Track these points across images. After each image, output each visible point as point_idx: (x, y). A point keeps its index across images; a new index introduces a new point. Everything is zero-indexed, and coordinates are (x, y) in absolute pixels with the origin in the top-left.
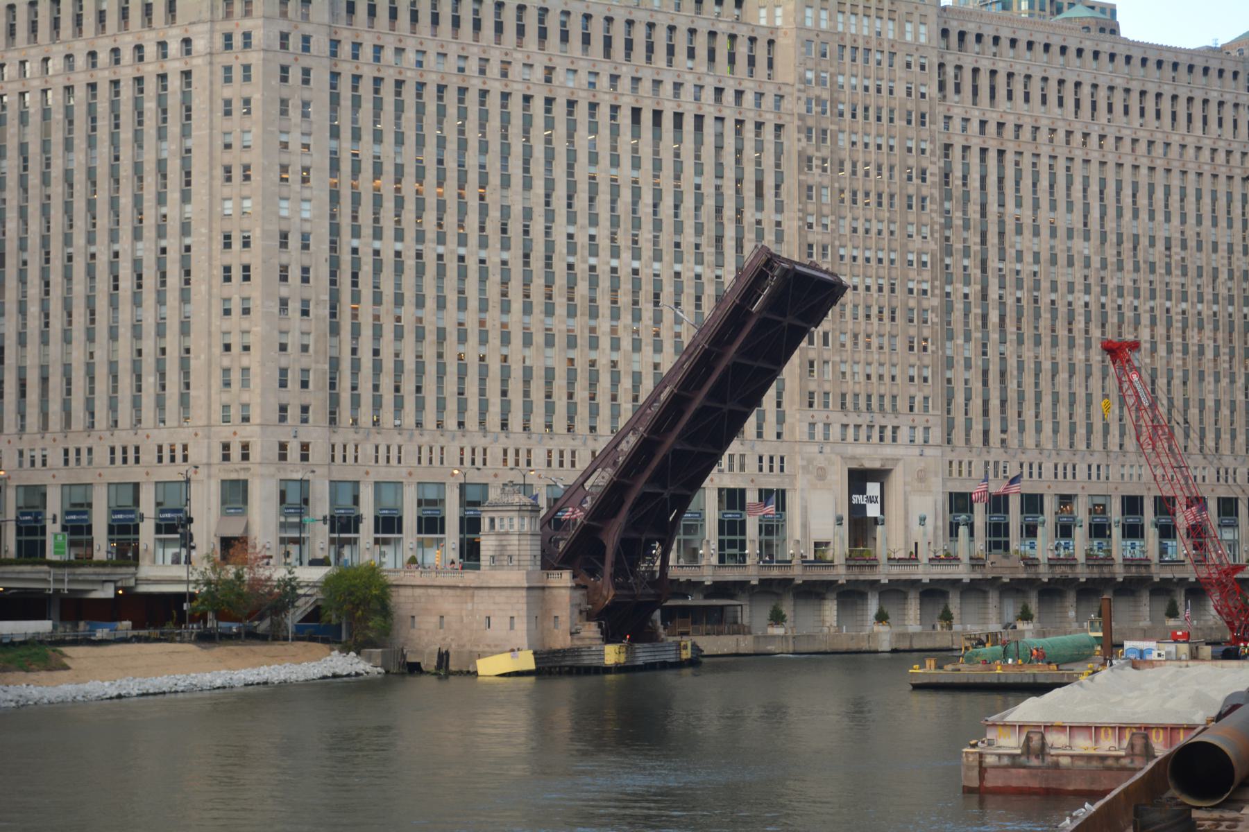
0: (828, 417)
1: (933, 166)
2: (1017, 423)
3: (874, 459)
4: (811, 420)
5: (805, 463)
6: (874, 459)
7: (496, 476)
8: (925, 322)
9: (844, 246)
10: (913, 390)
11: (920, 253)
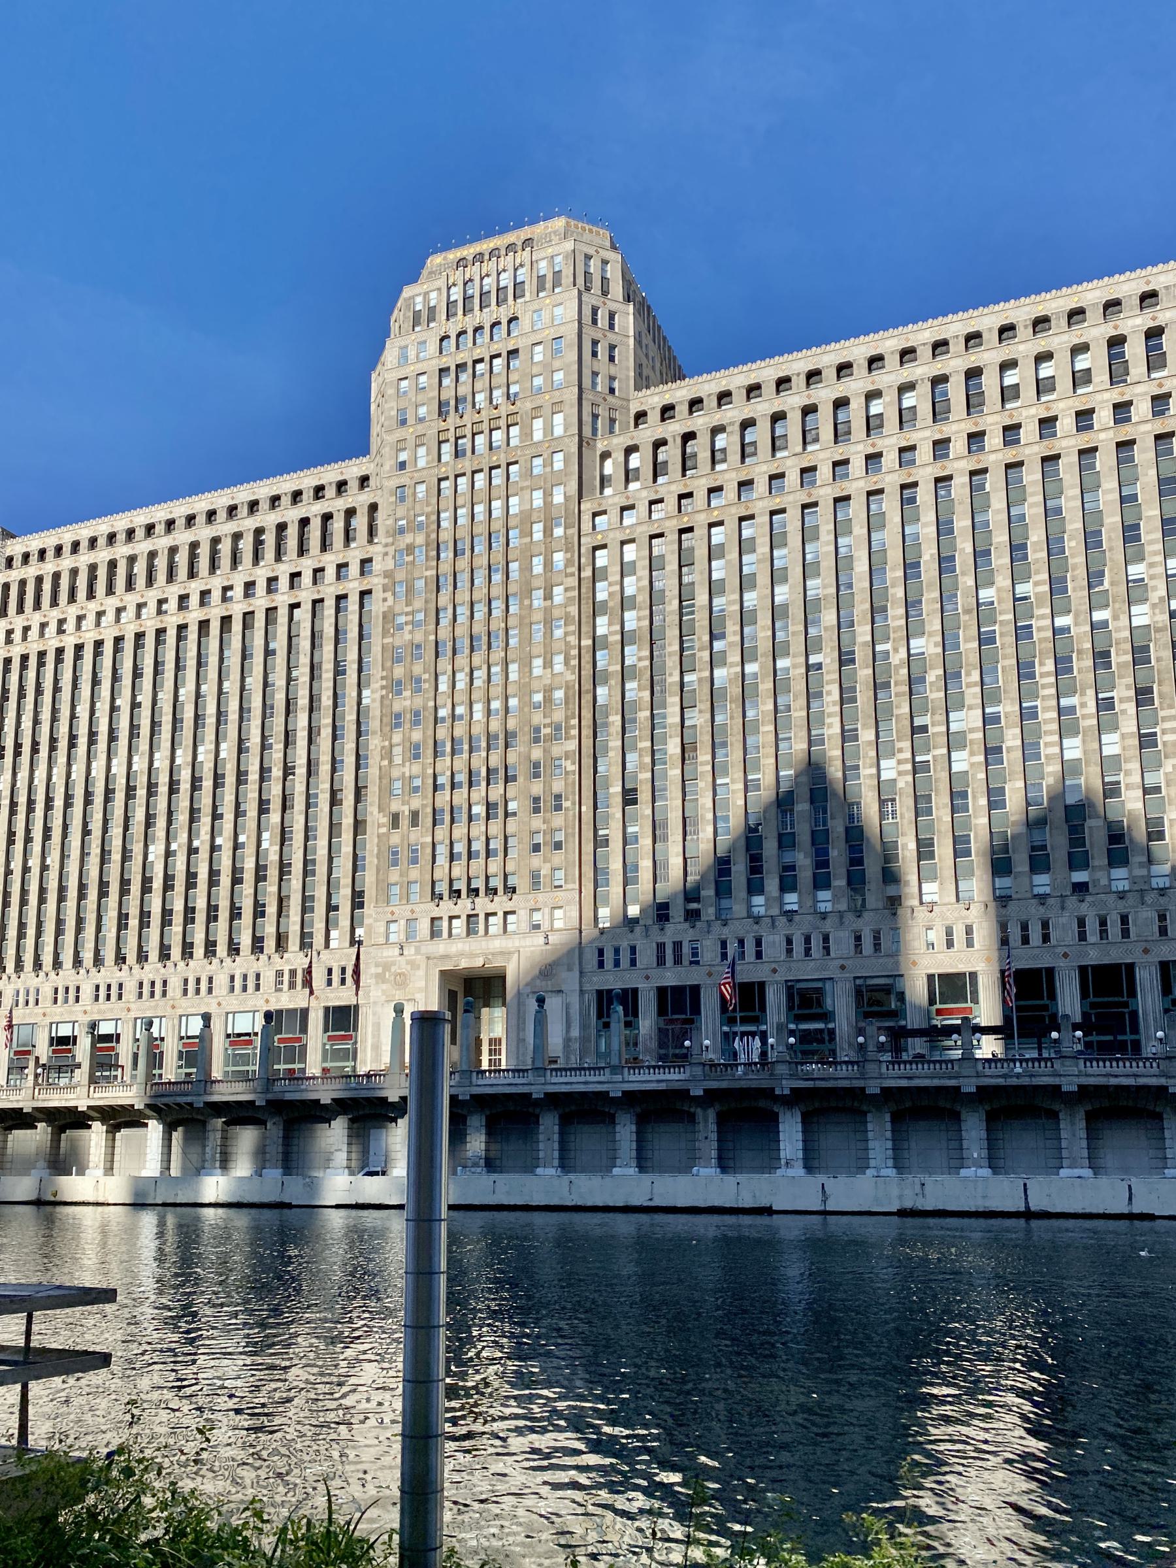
0: (413, 912)
1: (570, 579)
2: (713, 886)
3: (477, 955)
4: (389, 917)
5: (380, 970)
6: (477, 955)
9: (444, 706)
10: (536, 861)
11: (548, 691)
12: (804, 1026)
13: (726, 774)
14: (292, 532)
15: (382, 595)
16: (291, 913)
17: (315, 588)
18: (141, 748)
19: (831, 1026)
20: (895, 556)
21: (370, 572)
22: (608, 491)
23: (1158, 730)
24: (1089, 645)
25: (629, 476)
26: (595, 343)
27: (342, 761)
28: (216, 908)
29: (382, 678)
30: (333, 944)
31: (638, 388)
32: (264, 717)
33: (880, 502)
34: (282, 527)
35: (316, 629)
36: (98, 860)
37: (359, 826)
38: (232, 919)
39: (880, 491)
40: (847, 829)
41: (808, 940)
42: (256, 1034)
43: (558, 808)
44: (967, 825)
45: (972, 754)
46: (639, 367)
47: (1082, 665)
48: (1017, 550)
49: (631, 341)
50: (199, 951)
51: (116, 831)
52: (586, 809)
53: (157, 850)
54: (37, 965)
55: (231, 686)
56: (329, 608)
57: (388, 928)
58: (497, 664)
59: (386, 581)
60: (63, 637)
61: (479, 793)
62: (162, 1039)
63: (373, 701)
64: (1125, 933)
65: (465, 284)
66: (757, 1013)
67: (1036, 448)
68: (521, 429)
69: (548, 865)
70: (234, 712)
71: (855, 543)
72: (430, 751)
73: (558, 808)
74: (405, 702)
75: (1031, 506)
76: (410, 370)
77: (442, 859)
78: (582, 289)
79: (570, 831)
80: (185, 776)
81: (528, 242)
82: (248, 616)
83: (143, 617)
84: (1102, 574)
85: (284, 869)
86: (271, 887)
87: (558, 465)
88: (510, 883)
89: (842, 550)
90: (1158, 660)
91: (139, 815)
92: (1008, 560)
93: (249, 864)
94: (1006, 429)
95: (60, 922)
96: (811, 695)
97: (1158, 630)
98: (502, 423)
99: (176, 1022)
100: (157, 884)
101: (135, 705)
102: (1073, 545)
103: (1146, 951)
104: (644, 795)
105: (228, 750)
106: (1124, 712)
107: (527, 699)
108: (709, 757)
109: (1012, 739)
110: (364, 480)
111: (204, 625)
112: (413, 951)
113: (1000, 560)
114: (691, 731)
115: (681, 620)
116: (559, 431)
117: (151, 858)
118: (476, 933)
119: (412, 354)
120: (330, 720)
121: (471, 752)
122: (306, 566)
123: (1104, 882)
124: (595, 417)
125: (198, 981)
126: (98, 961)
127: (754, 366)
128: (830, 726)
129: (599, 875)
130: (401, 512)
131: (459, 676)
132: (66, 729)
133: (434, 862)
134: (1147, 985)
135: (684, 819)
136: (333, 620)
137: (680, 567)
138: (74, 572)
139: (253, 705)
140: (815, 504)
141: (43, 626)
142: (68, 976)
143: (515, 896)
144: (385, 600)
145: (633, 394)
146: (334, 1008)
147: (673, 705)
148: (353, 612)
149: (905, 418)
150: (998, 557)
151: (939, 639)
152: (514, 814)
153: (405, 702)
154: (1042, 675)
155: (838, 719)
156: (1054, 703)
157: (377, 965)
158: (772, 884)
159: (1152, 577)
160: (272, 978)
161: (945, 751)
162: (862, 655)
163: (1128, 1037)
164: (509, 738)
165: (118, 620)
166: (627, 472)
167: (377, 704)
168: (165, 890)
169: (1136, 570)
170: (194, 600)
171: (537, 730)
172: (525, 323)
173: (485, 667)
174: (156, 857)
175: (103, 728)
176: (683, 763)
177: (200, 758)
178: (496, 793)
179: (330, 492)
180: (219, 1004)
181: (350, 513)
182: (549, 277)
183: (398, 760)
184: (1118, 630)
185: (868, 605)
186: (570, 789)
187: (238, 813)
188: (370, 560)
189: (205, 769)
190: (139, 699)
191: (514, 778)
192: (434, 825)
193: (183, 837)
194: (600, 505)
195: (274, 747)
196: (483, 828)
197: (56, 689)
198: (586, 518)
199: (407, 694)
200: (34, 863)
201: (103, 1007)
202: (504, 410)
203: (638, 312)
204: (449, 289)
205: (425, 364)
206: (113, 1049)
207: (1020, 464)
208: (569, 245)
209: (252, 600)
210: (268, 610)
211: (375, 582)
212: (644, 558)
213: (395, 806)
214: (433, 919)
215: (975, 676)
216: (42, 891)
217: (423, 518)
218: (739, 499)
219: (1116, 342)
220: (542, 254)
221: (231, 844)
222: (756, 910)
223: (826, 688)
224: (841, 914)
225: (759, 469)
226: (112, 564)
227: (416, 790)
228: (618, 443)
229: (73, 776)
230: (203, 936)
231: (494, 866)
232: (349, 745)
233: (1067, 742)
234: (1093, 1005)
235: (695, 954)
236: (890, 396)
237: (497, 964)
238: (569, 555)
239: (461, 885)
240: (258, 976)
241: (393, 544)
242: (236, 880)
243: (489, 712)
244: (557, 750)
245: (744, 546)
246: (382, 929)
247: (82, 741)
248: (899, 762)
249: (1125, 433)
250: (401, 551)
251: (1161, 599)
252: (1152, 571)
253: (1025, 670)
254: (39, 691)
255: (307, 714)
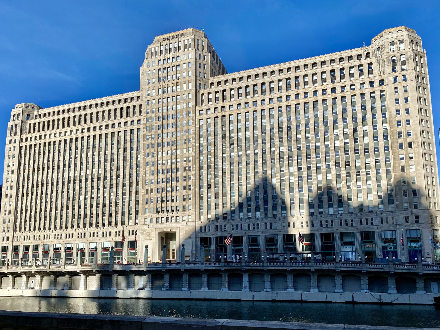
0: (151, 216)
1: (193, 128)
3: (169, 228)
4: (145, 217)
5: (143, 231)
6: (169, 228)
7: (52, 242)
8: (190, 179)
10: (184, 203)
12: (253, 247)
13: (233, 181)
14: (119, 111)
15: (143, 130)
16: (119, 216)
17: (125, 127)
18: (77, 170)
19: (259, 247)
20: (276, 126)
21: (140, 123)
22: (203, 104)
23: (341, 173)
24: (324, 151)
25: (209, 100)
26: (200, 64)
27: (132, 175)
28: (99, 213)
29: (143, 153)
30: (130, 224)
31: (211, 76)
32: (111, 162)
33: (273, 111)
34: (116, 110)
35: (125, 138)
36: (66, 200)
37: (137, 192)
38: (103, 217)
39: (273, 108)
40: (264, 196)
41: (254, 225)
42: (110, 248)
43: (190, 189)
44: (293, 196)
45: (295, 178)
46: (212, 70)
47: (322, 156)
48: (307, 125)
49: (210, 63)
50: (94, 225)
51: (71, 192)
52: (198, 189)
53: (82, 198)
54: (50, 228)
55: (102, 153)
56: (129, 133)
57: (145, 220)
58: (174, 150)
59: (144, 126)
60: (55, 138)
61: (169, 184)
62: (84, 249)
63: (141, 158)
64: (332, 225)
65: (165, 45)
66: (241, 244)
67: (312, 99)
68: (180, 87)
69: (187, 204)
70: (103, 160)
71: (266, 121)
72: (156, 173)
73: (190, 189)
74: (149, 159)
75: (310, 114)
76: (150, 69)
77: (159, 202)
78: (197, 49)
79: (193, 195)
80: (90, 177)
81: (182, 35)
82: (107, 134)
83: (78, 133)
84: (328, 132)
85: (117, 204)
86: (113, 208)
87: (190, 97)
88: (177, 209)
89: (263, 123)
90: (341, 155)
91: (77, 188)
92: (304, 128)
93: (107, 202)
94: (304, 93)
95: (56, 217)
96: (255, 161)
97: (341, 147)
98: (175, 85)
99: (88, 244)
100: (82, 207)
101: (76, 157)
102: (321, 124)
103: (337, 230)
104: (213, 186)
105: (101, 170)
106: (332, 168)
107: (182, 159)
108: (229, 177)
109: (305, 174)
110: (138, 97)
111: (94, 136)
112: (151, 227)
113: (303, 128)
114: (224, 169)
115: (222, 140)
116: (190, 88)
117: (81, 199)
118: (168, 222)
119: (151, 64)
120: (129, 163)
121: (167, 173)
122: (123, 121)
123: (327, 212)
124: (200, 84)
125: (94, 233)
126: (67, 227)
127: (241, 72)
128: (260, 169)
129: (201, 207)
130: (148, 107)
131: (164, 153)
132: (57, 164)
133: (157, 202)
134: (337, 238)
135: (223, 192)
136: (130, 136)
137: (222, 126)
138: (58, 120)
139: (108, 159)
140: (256, 111)
141: (50, 135)
142: (58, 231)
143: (179, 212)
144: (144, 131)
145: (210, 78)
146: (131, 241)
147: (220, 162)
148: (135, 134)
149: (280, 88)
150: (302, 127)
151: (287, 148)
152: (179, 190)
153: (149, 159)
154: (313, 158)
155: (262, 168)
156: (315, 165)
157: (142, 230)
158: (245, 210)
159: (340, 134)
160: (114, 232)
161: (288, 177)
162: (268, 151)
163: (332, 251)
164: (177, 170)
165: (71, 134)
166: (208, 99)
167: (142, 159)
168: (85, 209)
169: (336, 132)
170: (92, 129)
171: (185, 168)
172: (181, 57)
173: (171, 150)
174: (82, 199)
175: (67, 164)
176: (223, 178)
177: (94, 173)
178: (174, 184)
179: (129, 100)
180: (100, 240)
181: (134, 107)
182: (188, 45)
183: (147, 175)
184: (331, 147)
185: (269, 138)
186: (193, 184)
187: (104, 188)
188: (140, 120)
189: (95, 176)
190: (77, 156)
191: (179, 181)
192: (157, 192)
193: (89, 194)
194: (201, 108)
195: (114, 170)
196: (170, 194)
197: (54, 152)
198: (198, 112)
199: (150, 157)
200: (48, 200)
201: (68, 240)
202: (176, 81)
203: (212, 55)
204: (161, 46)
205: (155, 67)
206: (71, 251)
207: (308, 103)
208: (193, 37)
209: (108, 130)
210: (112, 133)
211: (141, 126)
212: (213, 123)
213: (147, 187)
214: (157, 218)
215: (296, 158)
216: (51, 208)
217: (154, 109)
218: (237, 108)
219: (333, 71)
220: (186, 39)
221: (102, 197)
222: (241, 217)
223: (259, 159)
224: (262, 218)
225: (242, 100)
226: (69, 118)
227: (152, 183)
228: (206, 91)
229: (59, 177)
230: (95, 221)
231: (173, 204)
232: (134, 170)
233: (318, 176)
234: (324, 243)
235: (225, 228)
236: (276, 83)
237: (174, 230)
238: (193, 121)
239: (164, 209)
240: (110, 232)
241: (146, 116)
242: (104, 206)
243: (172, 163)
244: (190, 173)
245: (238, 121)
246: (143, 221)
247: (61, 167)
248: (277, 179)
249: (334, 96)
250: (148, 118)
251: (342, 139)
252: (340, 132)
253: (308, 157)
254: (49, 153)
255: (123, 162)
